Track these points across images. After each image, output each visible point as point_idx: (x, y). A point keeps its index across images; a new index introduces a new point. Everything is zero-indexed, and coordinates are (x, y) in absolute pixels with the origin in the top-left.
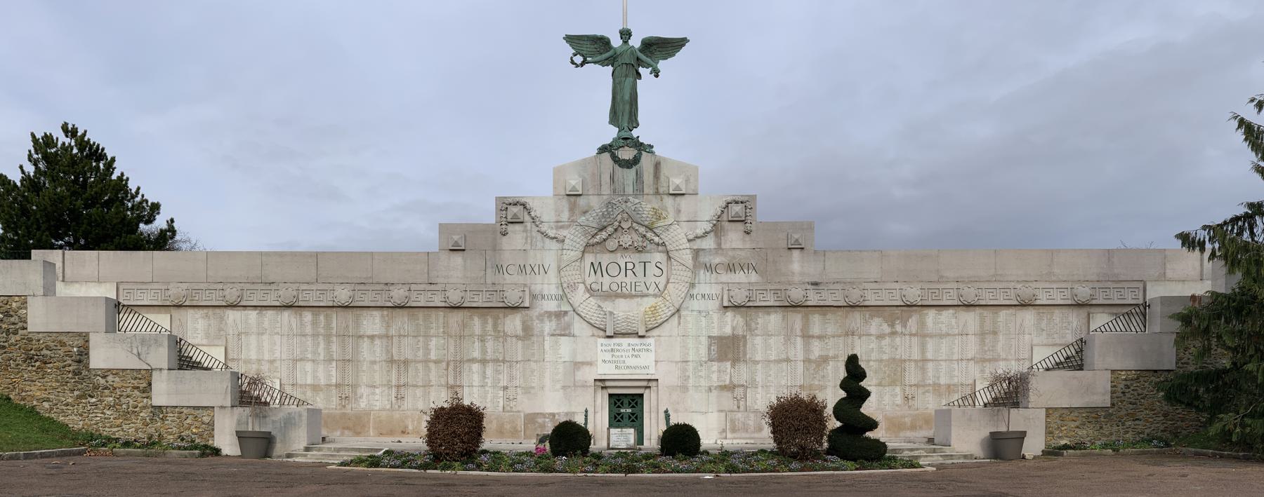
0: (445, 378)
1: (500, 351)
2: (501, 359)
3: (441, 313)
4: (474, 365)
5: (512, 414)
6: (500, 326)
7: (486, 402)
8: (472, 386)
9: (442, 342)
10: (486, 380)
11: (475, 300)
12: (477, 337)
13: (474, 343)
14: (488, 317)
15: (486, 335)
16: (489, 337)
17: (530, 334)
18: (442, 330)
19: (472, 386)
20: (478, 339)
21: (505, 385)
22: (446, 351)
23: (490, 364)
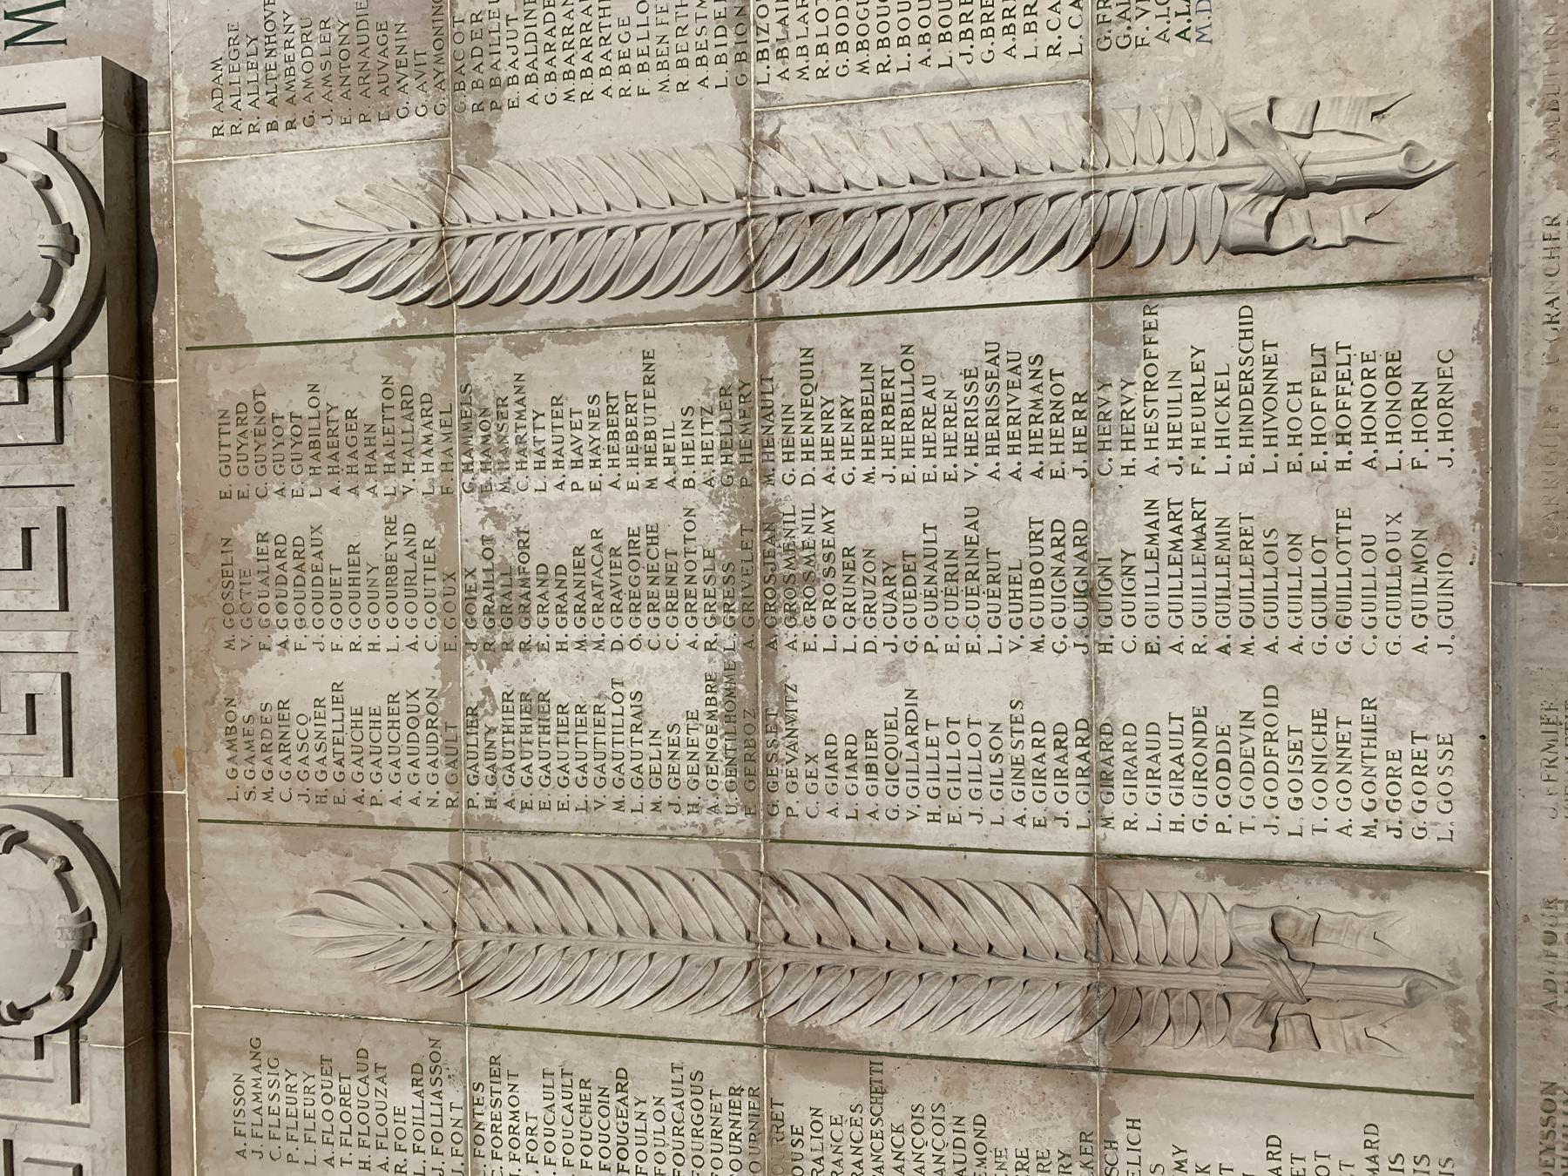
0: (981, 1097)
1: (635, 367)
2: (721, 362)
3: (221, 1085)
4: (804, 708)
5: (1531, 130)
6: (339, 395)
7: (1331, 540)
8: (1095, 730)
9: (531, 1096)
10: (1011, 546)
11: (47, 685)
12: (475, 677)
13: (534, 704)
14: (245, 533)
15: (438, 558)
16: (469, 510)
17: (418, 38)
18: (401, 1095)
19: (1095, 730)
20: (490, 652)
21: (1058, 281)
22: (648, 1062)
23: (791, 497)
